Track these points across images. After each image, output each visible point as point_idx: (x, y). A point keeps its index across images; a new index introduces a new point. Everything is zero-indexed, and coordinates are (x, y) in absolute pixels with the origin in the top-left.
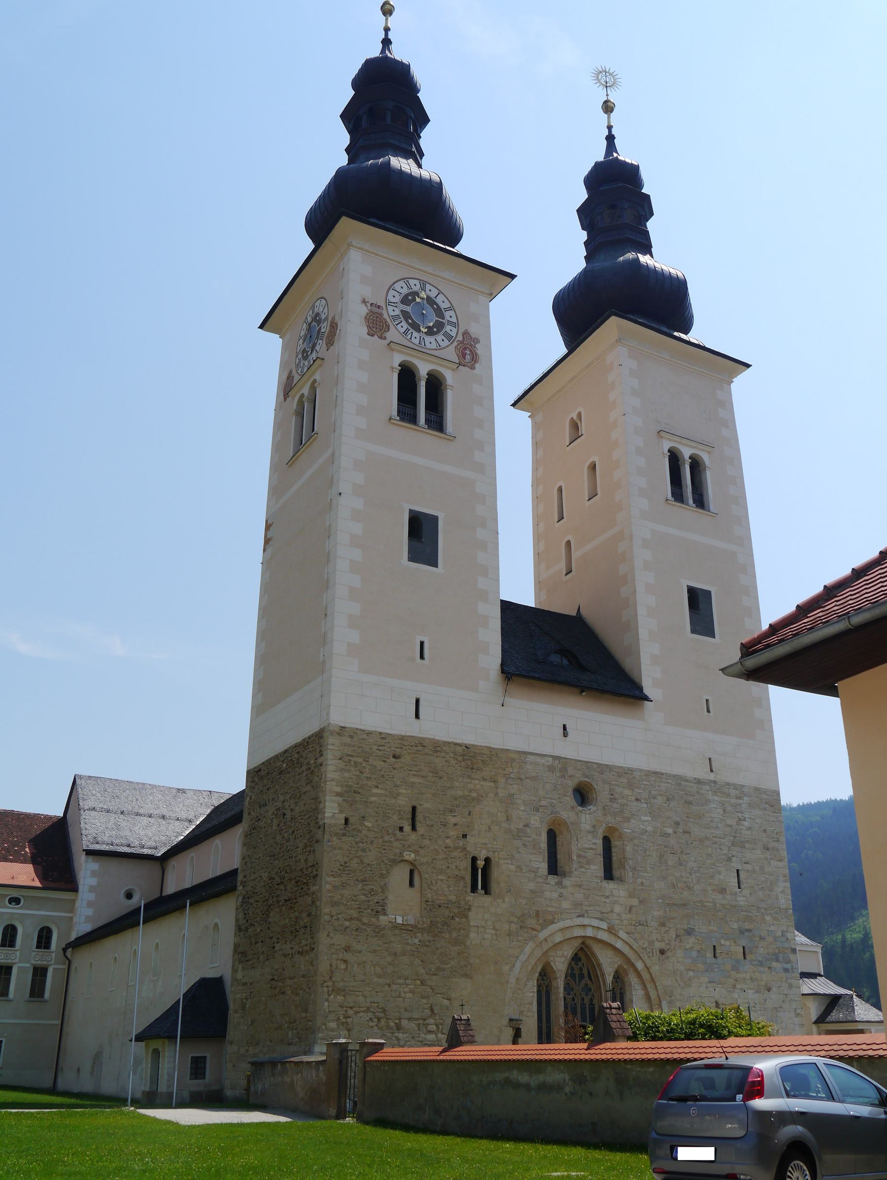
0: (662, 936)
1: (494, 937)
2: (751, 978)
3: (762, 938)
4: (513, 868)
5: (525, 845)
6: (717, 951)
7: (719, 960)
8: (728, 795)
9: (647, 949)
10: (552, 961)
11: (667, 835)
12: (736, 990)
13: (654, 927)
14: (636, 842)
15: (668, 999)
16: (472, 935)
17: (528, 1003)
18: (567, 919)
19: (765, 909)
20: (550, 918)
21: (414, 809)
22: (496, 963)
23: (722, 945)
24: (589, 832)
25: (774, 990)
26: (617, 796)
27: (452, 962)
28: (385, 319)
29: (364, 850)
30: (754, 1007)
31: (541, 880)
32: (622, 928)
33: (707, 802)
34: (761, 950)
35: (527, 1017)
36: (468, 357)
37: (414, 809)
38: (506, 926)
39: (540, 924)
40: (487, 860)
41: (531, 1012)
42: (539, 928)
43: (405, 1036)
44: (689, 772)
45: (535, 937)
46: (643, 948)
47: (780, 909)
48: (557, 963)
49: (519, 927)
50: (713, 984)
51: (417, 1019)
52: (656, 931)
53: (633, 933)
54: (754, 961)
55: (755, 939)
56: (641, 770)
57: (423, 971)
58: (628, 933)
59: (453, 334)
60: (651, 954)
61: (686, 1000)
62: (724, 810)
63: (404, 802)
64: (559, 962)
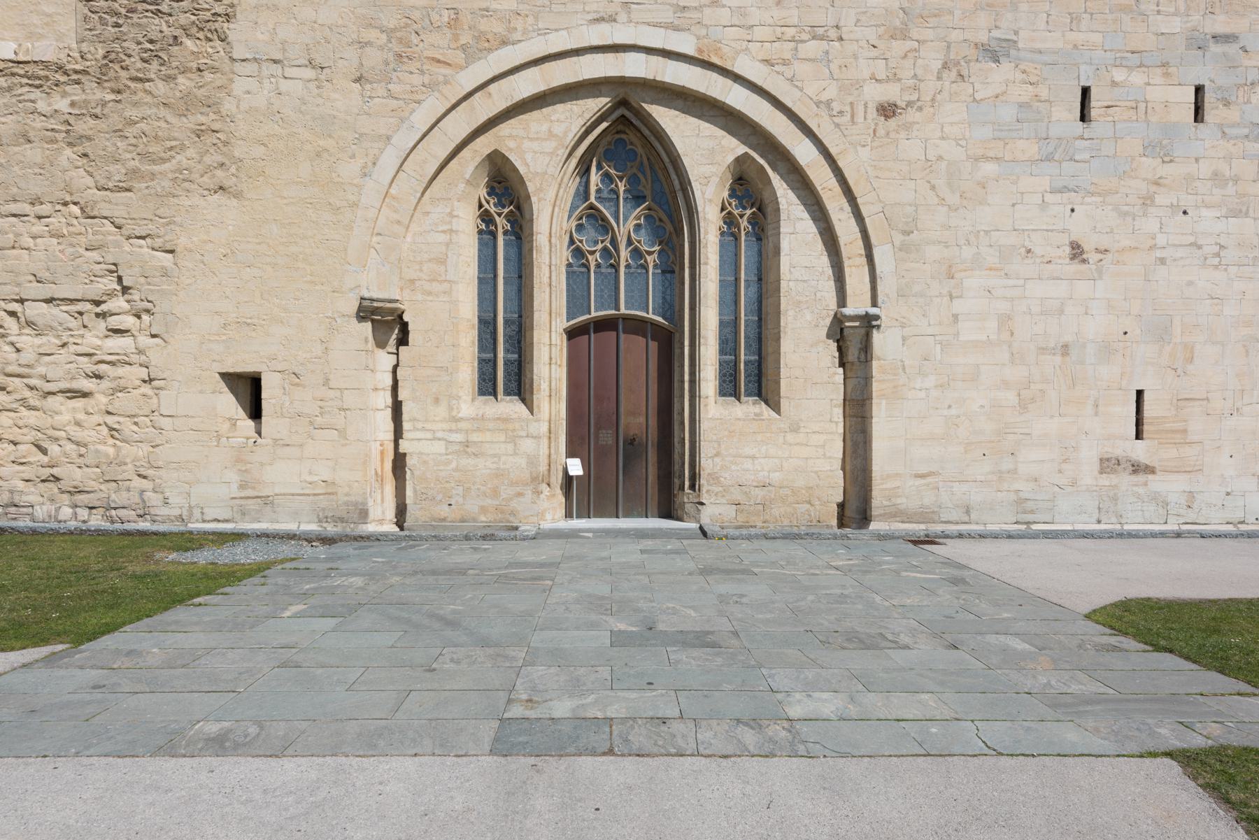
0: (891, 65)
1: (312, 86)
2: (1216, 175)
6: (1093, 104)
9: (834, 105)
10: (511, 150)
12: (1151, 210)
13: (863, 43)
15: (898, 238)
16: (239, 86)
17: (430, 260)
18: (556, 30)
20: (498, 28)
22: (318, 155)
23: (1114, 84)
27: (178, 157)
30: (1218, 255)
32: (747, 49)
35: (430, 293)
39: (464, 48)
41: (441, 282)
43: (38, 341)
45: (446, 83)
46: (818, 104)
48: (529, 157)
49: (391, 57)
50: (1066, 195)
51: (72, 301)
52: (875, 53)
53: (785, 63)
54: (1233, 126)
55: (1247, 63)
57: (89, 181)
58: (766, 61)
60: (847, 117)
61: (962, 242)
64: (535, 152)
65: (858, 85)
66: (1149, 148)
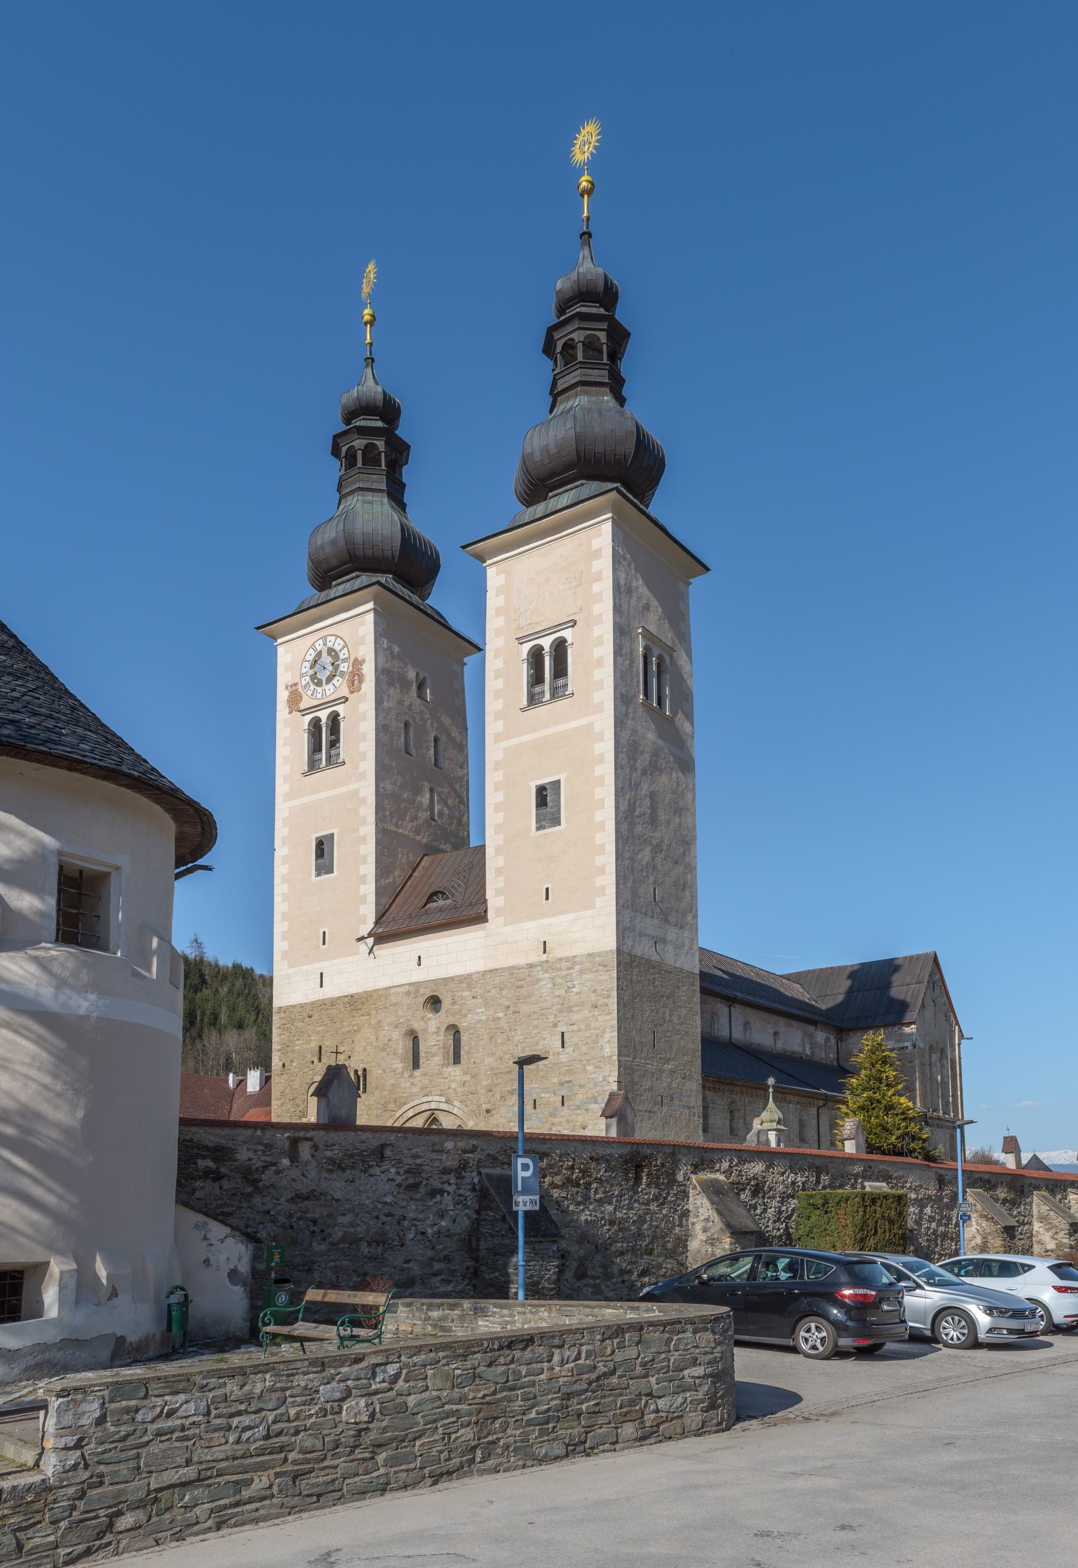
2: (568, 1121)
3: (581, 1086)
4: (380, 1071)
5: (388, 1054)
7: (538, 1110)
8: (560, 969)
11: (499, 1019)
14: (471, 1031)
19: (588, 1061)
20: (404, 1101)
21: (320, 1047)
24: (434, 1033)
25: (590, 1127)
26: (457, 999)
28: (300, 693)
29: (293, 1081)
31: (398, 1076)
33: (538, 980)
34: (580, 1096)
36: (356, 682)
37: (320, 1047)
38: (375, 1112)
40: (365, 1070)
42: (396, 1109)
44: (521, 960)
47: (604, 1057)
56: (478, 973)
59: (345, 670)
62: (554, 984)
63: (314, 1045)
65: (481, 1105)
66: (551, 1115)
